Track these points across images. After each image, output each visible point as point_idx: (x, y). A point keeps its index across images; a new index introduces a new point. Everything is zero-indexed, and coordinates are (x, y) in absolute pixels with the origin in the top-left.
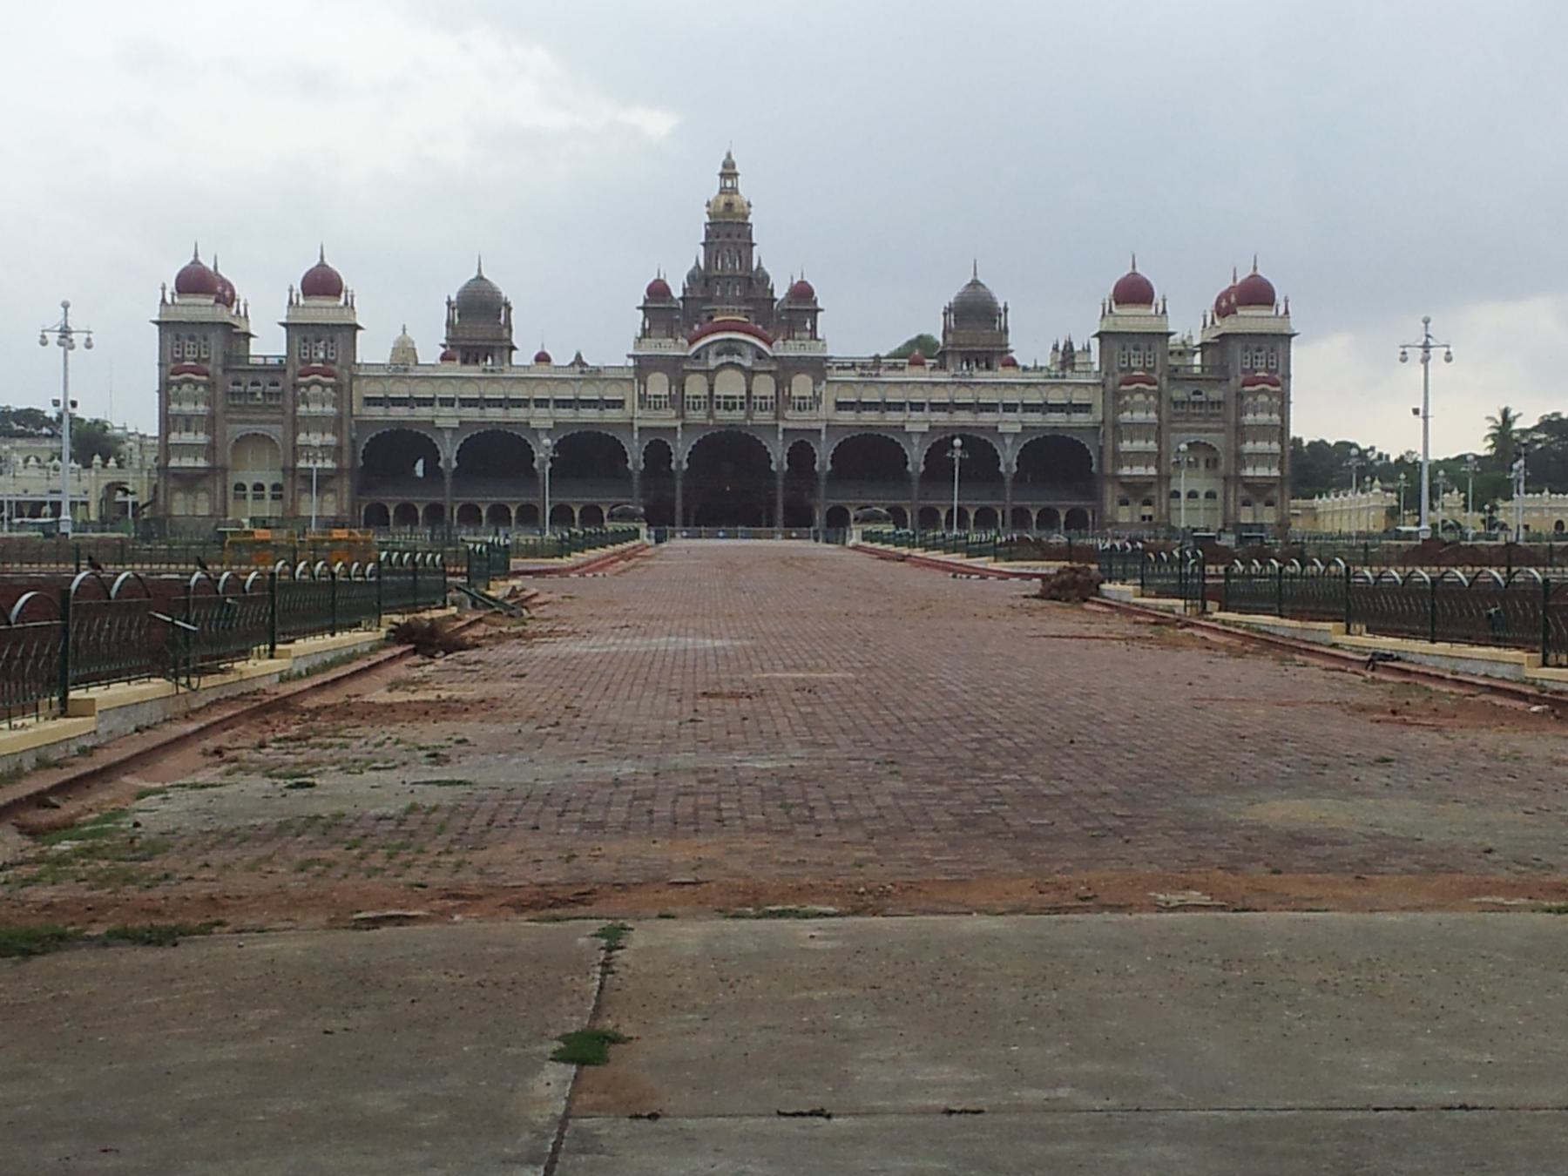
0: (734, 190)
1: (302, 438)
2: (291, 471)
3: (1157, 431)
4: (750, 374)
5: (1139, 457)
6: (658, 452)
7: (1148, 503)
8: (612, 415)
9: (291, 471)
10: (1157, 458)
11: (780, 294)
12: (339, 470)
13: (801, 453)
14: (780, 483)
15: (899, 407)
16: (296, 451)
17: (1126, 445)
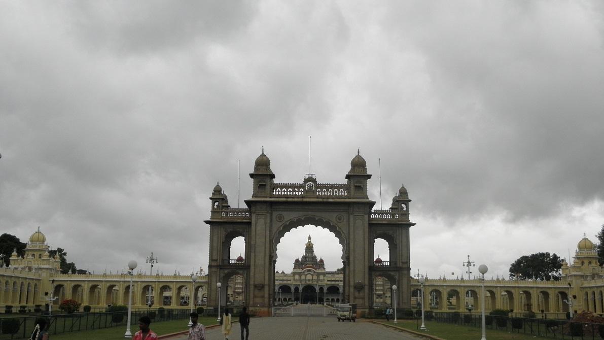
0: (311, 242)
1: (236, 286)
2: (234, 292)
3: (383, 285)
4: (312, 275)
5: (379, 290)
6: (297, 289)
7: (381, 298)
8: (289, 282)
9: (234, 292)
10: (383, 290)
11: (318, 260)
12: (242, 292)
13: (321, 289)
14: (318, 294)
15: (338, 281)
16: (235, 288)
17: (377, 288)
